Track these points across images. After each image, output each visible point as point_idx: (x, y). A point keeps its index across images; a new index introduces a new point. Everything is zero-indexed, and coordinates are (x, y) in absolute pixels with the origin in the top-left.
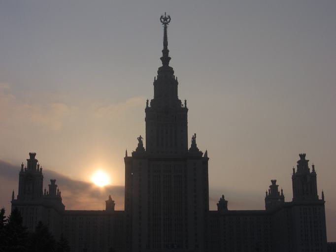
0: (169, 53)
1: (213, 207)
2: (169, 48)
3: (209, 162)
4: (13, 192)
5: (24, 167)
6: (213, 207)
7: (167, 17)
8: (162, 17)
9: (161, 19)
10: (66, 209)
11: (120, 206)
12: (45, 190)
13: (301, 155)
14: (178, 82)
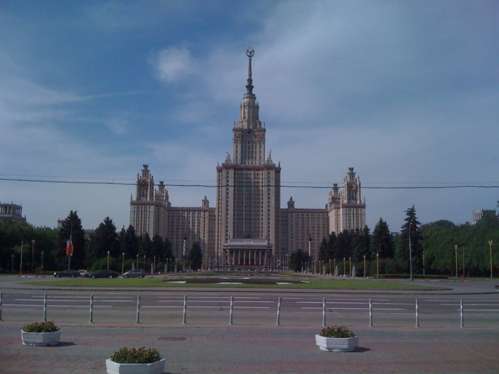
1: (284, 205)
2: (253, 78)
3: (281, 171)
4: (132, 195)
6: (284, 205)
8: (247, 50)
9: (247, 53)
10: (172, 206)
11: (213, 204)
12: (156, 190)
13: (349, 169)
14: (259, 106)
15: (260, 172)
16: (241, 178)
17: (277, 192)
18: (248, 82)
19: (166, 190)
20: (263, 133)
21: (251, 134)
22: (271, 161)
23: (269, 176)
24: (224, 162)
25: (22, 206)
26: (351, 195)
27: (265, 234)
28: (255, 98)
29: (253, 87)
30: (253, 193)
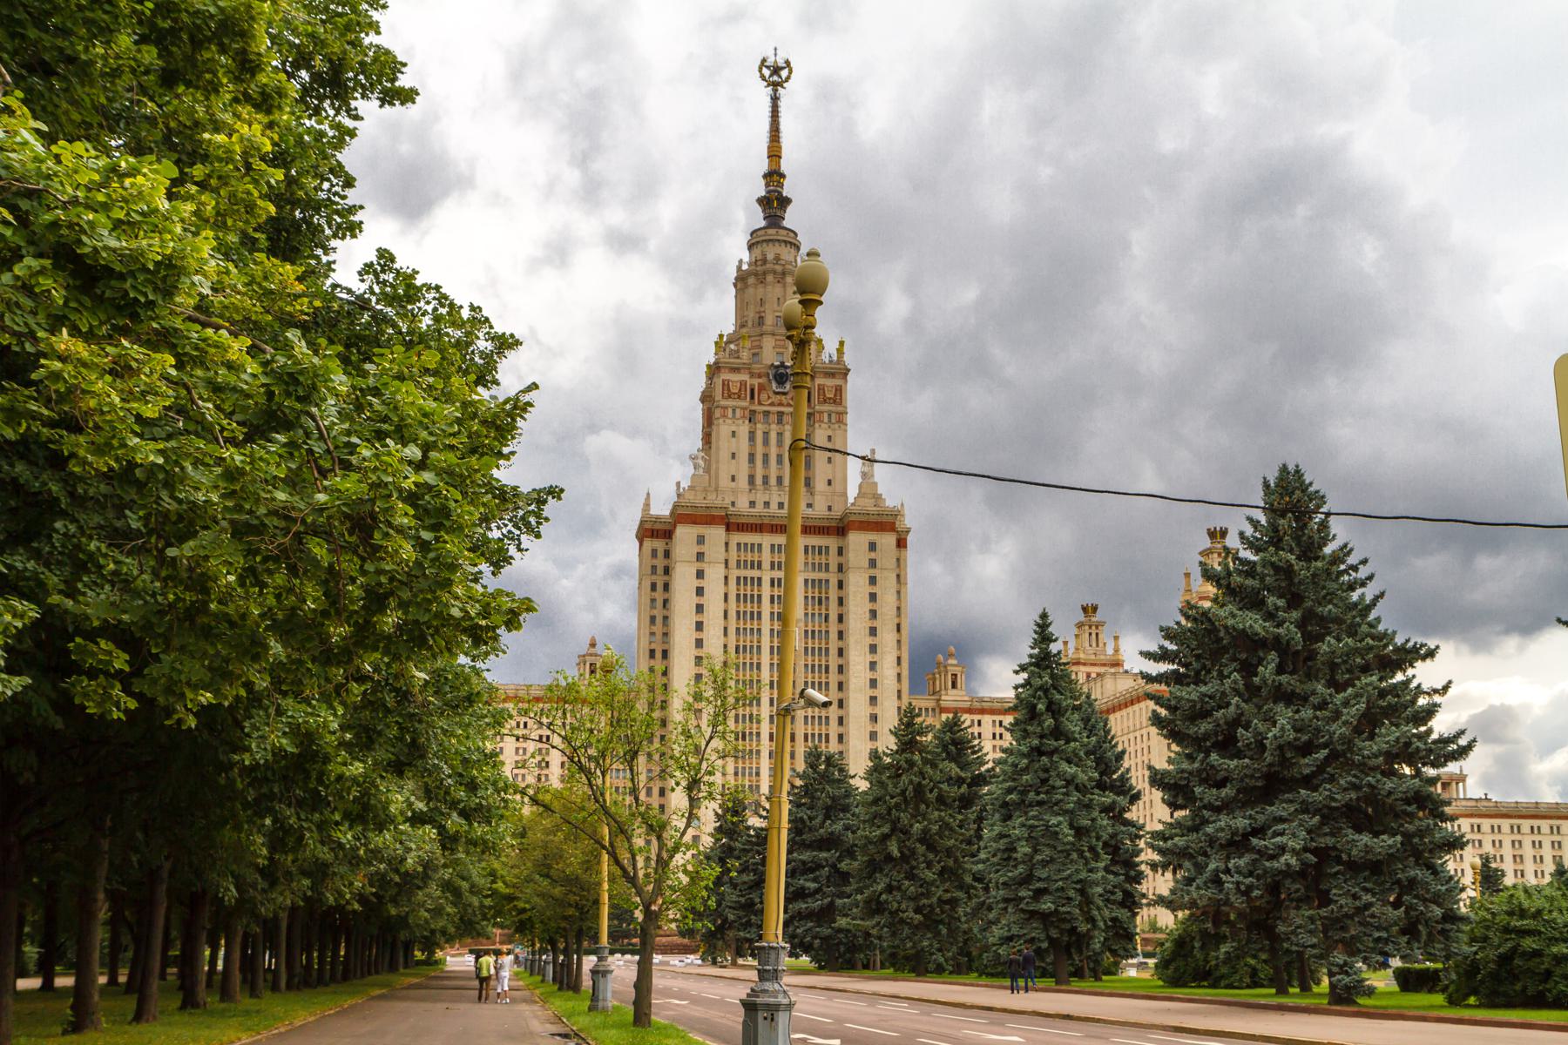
0: (786, 183)
2: (785, 167)
7: (781, 63)
8: (764, 60)
13: (1212, 534)
15: (831, 542)
16: (752, 567)
18: (767, 185)
20: (838, 382)
21: (788, 386)
22: (877, 497)
23: (873, 555)
29: (787, 201)
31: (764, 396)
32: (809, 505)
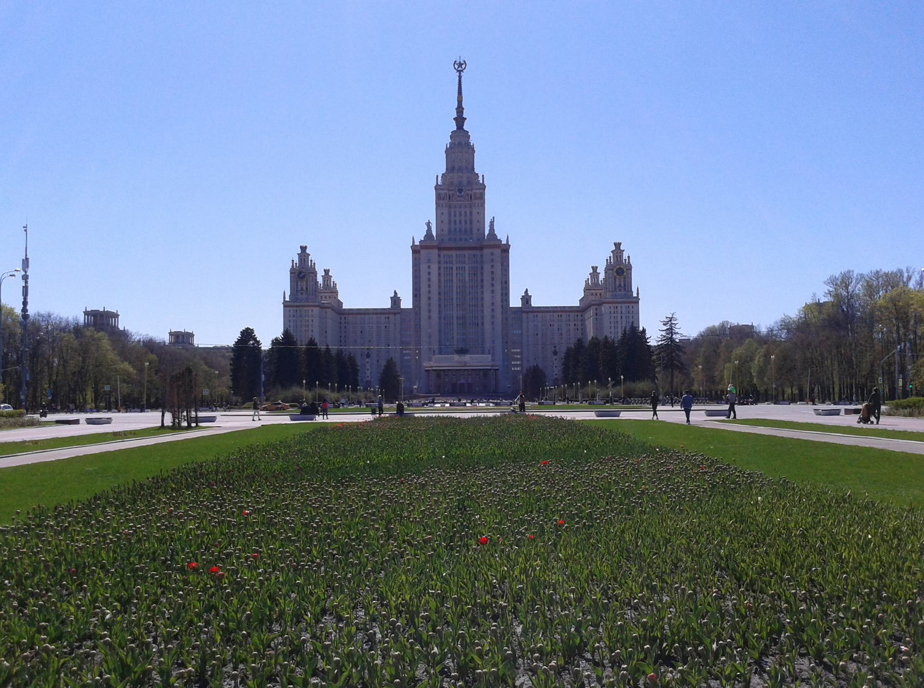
1: (515, 302)
5: (295, 262)
6: (515, 302)
7: (462, 62)
8: (455, 62)
10: (345, 306)
11: (407, 303)
13: (615, 244)
15: (478, 252)
17: (504, 282)
18: (457, 113)
19: (333, 282)
20: (483, 191)
21: (463, 193)
23: (492, 257)
24: (423, 239)
25: (119, 313)
26: (617, 283)
27: (488, 345)
28: (469, 137)
30: (467, 284)
31: (454, 198)
32: (471, 239)
